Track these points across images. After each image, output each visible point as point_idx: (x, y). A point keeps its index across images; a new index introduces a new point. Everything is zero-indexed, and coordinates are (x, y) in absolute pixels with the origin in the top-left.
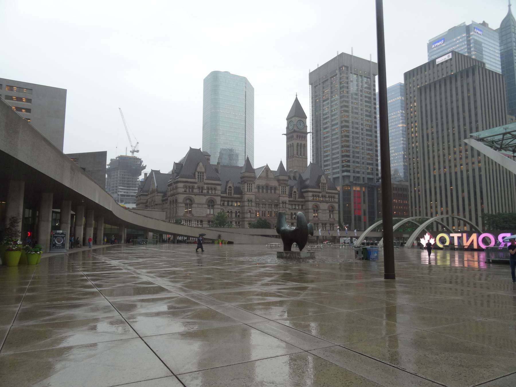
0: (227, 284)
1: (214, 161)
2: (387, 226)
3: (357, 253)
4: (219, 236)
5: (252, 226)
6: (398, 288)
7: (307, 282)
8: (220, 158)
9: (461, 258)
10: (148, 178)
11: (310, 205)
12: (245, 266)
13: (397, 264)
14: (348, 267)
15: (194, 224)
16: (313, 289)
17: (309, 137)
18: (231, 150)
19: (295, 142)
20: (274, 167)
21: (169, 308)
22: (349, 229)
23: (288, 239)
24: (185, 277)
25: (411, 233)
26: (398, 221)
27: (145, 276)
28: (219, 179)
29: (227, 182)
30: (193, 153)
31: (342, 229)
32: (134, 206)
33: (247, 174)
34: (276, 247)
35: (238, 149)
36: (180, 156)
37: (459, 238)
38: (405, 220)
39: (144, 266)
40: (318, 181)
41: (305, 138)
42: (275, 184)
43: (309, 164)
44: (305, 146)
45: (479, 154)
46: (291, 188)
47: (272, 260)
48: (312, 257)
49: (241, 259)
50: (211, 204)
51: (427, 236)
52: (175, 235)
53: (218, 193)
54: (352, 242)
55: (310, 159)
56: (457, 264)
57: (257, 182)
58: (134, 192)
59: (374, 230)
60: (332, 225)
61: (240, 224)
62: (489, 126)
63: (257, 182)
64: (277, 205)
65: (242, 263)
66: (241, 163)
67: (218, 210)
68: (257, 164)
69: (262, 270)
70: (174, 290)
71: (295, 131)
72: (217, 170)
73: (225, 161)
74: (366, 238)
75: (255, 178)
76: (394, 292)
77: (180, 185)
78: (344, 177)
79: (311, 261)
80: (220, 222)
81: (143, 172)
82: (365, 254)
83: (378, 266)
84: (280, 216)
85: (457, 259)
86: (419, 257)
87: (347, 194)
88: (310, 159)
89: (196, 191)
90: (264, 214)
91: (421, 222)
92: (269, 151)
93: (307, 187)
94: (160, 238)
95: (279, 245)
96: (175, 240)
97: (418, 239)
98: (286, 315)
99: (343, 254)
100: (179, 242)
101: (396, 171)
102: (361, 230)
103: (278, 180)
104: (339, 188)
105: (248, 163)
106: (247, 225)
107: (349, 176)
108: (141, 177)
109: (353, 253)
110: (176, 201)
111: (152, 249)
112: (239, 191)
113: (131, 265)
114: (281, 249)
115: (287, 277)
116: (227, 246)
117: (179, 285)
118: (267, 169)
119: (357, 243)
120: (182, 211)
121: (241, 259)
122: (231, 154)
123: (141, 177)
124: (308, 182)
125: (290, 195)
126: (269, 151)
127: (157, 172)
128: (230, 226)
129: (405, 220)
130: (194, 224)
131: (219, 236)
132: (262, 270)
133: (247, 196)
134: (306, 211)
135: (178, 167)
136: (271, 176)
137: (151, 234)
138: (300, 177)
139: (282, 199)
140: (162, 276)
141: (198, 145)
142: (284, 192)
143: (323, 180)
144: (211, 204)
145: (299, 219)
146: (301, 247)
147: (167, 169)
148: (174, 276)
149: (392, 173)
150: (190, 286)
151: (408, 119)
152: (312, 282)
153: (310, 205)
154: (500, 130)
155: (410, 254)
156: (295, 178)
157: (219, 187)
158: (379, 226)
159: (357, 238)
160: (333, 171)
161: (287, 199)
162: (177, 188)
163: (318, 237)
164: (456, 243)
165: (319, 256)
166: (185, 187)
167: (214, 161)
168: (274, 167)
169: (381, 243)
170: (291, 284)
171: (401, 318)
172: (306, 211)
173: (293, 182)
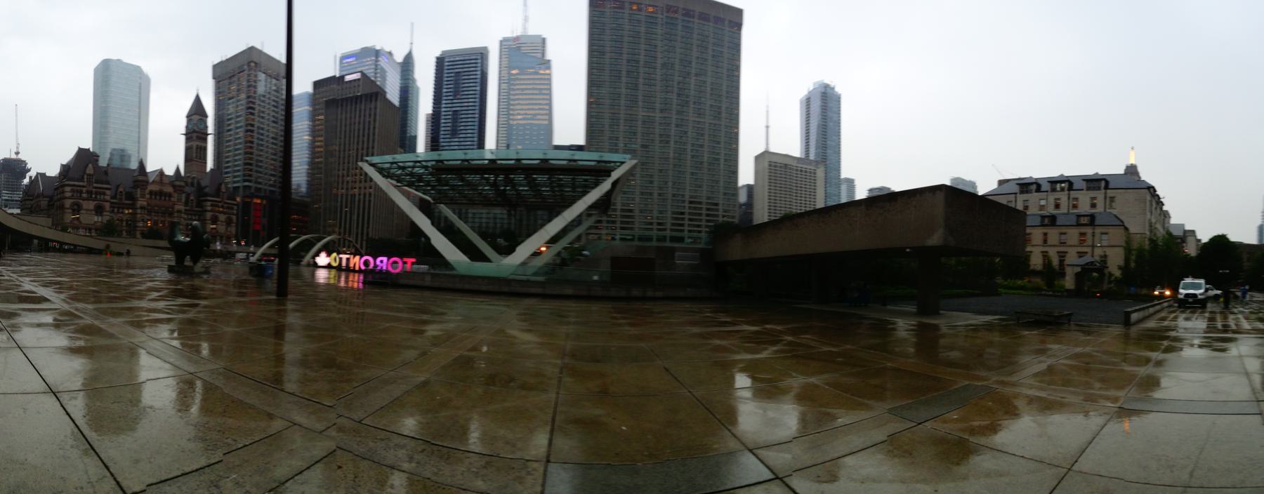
0: (115, 298)
1: (103, 162)
2: (282, 245)
3: (251, 269)
4: (108, 247)
5: (144, 236)
6: (290, 306)
7: (199, 298)
8: (110, 159)
9: (347, 278)
10: (33, 182)
11: (209, 215)
12: (135, 279)
13: (291, 281)
14: (241, 284)
15: (81, 232)
16: (206, 307)
17: (210, 140)
18: (123, 150)
19: (195, 144)
20: (170, 171)
21: (55, 320)
22: (247, 244)
23: (180, 250)
24: (71, 288)
25: (308, 251)
26: (295, 238)
27: (27, 285)
28: (108, 183)
29: (118, 187)
30: (82, 153)
31: (238, 244)
32: (18, 211)
33: (141, 178)
34: (169, 260)
35: (131, 149)
36: (68, 156)
37: (348, 259)
38: (304, 237)
39: (28, 274)
40: (219, 189)
41: (205, 140)
42: (169, 189)
43: (208, 169)
44: (205, 149)
45: (371, 180)
46: (188, 195)
47: (162, 274)
48: (207, 272)
49: (131, 272)
50: (99, 210)
51: (323, 255)
52: (62, 243)
53: (108, 198)
54: (248, 258)
55: (210, 165)
56: (342, 284)
57: (150, 188)
58: (18, 196)
59: (271, 247)
60: (229, 239)
61: (131, 233)
62: (382, 153)
63: (150, 188)
64: (171, 214)
65: (132, 276)
66: (134, 165)
67: (106, 218)
68: (151, 167)
69: (150, 284)
70: (57, 300)
71: (194, 131)
72: (106, 173)
73: (116, 163)
74: (264, 255)
75: (147, 182)
76: (285, 311)
77: (68, 189)
78: (245, 187)
79: (205, 276)
80: (108, 230)
81: (28, 175)
82: (258, 271)
83: (271, 285)
84: (173, 225)
85: (343, 279)
86: (313, 275)
87: (246, 206)
88: (210, 165)
89: (84, 195)
90: (156, 223)
91: (319, 240)
92: (165, 153)
93: (206, 195)
94: (45, 246)
95: (170, 258)
96: (62, 249)
97: (314, 257)
98: (176, 335)
99: (238, 268)
100: (66, 251)
101: (299, 186)
102: (258, 246)
103: (174, 186)
104: (238, 199)
105: (142, 166)
106: (138, 235)
107: (249, 187)
108: (26, 181)
109: (247, 269)
110: (62, 207)
111: (38, 257)
112: (131, 197)
113: (14, 272)
114: (173, 263)
115: (177, 293)
116: (116, 258)
117: (62, 296)
118: (161, 173)
119: (253, 259)
120: (69, 217)
121: (131, 272)
122: (123, 155)
123: (26, 181)
124: (207, 190)
125: (186, 204)
126: (165, 153)
127: (43, 175)
128: (120, 235)
129: (304, 237)
130: (81, 232)
131: (108, 247)
132: (150, 284)
133: (141, 202)
134: (203, 221)
135: (65, 169)
136: (166, 181)
137: (36, 241)
138: (199, 183)
139: (177, 207)
140: (46, 285)
141: (88, 144)
142: (179, 200)
143: (223, 188)
144: (99, 210)
145: (194, 228)
146: (195, 261)
147: (53, 171)
148: (59, 287)
149: (294, 187)
150: (74, 298)
151: (314, 132)
152: (206, 298)
153: (209, 215)
154: (388, 158)
155: (305, 271)
156: (192, 184)
157: (108, 192)
158: (276, 243)
159: (254, 254)
160: (233, 180)
161: (182, 208)
162: (63, 192)
163: (215, 251)
164: (344, 263)
165: (216, 271)
166: (72, 191)
167: (103, 162)
168: (170, 171)
169: (277, 261)
170: (181, 301)
171: (289, 336)
172: (203, 221)
173: (190, 188)
